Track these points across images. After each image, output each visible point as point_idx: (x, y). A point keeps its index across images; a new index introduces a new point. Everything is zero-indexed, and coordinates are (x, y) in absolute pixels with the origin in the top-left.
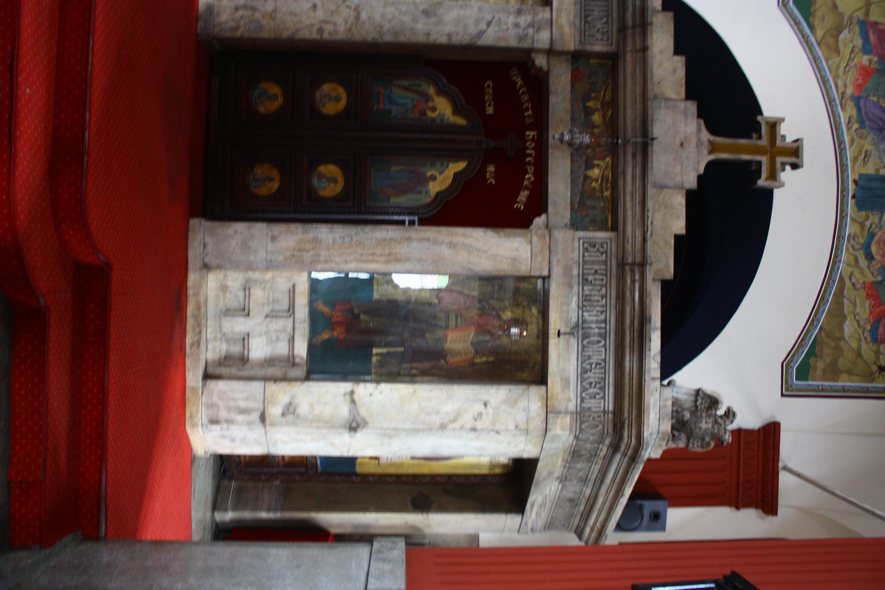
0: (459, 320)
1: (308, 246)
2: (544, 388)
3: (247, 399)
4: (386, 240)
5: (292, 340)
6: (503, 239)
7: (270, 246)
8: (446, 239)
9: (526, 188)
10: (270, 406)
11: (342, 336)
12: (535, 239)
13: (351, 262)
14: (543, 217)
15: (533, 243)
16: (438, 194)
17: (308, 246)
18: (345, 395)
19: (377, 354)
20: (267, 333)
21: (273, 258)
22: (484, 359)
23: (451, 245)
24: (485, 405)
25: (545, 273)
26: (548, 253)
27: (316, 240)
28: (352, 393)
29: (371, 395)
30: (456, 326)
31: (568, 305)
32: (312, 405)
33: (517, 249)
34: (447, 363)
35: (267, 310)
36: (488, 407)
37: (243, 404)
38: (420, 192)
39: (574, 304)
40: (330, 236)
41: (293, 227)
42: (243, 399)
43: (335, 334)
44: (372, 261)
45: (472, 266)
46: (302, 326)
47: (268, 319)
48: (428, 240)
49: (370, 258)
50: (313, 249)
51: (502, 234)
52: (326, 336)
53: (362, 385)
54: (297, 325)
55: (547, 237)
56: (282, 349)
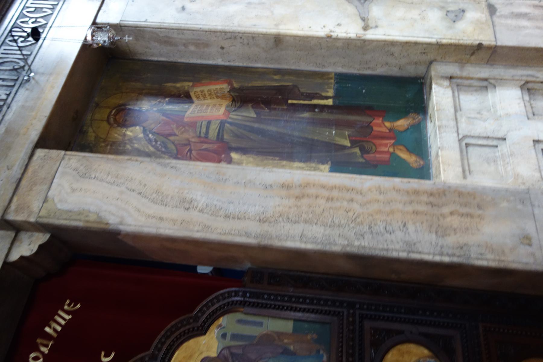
0: (204, 130)
1: (455, 221)
2: (98, 20)
3: (520, 28)
4: (306, 222)
5: (457, 109)
6: (93, 208)
7: (530, 228)
8: (194, 215)
9: (48, 337)
10: (484, 19)
11: (379, 121)
12: (36, 205)
13: (370, 190)
14: (14, 257)
15: (41, 199)
16: (203, 330)
17: (455, 221)
18: (376, 27)
19: (327, 98)
20: (498, 118)
21: (520, 207)
22: (178, 85)
23: (187, 204)
24: (183, 8)
25: (40, 153)
26: (23, 182)
27: (442, 231)
28: (366, 28)
29: (339, 25)
30: (209, 123)
31: (23, 107)
32: (423, 19)
33: (74, 190)
34: (230, 83)
35: (504, 148)
36: (181, 6)
37: (524, 23)
38: (235, 337)
39: (15, 107)
40: (413, 236)
41: (488, 260)
42: (525, 27)
43: (388, 124)
44: (332, 188)
45: (159, 169)
46: (444, 122)
47: (500, 135)
48: (227, 216)
49: (335, 193)
50: (444, 216)
51: (92, 218)
52: (402, 123)
53: (353, 35)
54: (453, 123)
55: (13, 206)
56: (470, 101)
